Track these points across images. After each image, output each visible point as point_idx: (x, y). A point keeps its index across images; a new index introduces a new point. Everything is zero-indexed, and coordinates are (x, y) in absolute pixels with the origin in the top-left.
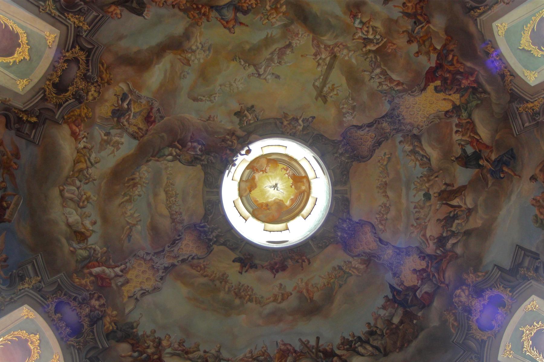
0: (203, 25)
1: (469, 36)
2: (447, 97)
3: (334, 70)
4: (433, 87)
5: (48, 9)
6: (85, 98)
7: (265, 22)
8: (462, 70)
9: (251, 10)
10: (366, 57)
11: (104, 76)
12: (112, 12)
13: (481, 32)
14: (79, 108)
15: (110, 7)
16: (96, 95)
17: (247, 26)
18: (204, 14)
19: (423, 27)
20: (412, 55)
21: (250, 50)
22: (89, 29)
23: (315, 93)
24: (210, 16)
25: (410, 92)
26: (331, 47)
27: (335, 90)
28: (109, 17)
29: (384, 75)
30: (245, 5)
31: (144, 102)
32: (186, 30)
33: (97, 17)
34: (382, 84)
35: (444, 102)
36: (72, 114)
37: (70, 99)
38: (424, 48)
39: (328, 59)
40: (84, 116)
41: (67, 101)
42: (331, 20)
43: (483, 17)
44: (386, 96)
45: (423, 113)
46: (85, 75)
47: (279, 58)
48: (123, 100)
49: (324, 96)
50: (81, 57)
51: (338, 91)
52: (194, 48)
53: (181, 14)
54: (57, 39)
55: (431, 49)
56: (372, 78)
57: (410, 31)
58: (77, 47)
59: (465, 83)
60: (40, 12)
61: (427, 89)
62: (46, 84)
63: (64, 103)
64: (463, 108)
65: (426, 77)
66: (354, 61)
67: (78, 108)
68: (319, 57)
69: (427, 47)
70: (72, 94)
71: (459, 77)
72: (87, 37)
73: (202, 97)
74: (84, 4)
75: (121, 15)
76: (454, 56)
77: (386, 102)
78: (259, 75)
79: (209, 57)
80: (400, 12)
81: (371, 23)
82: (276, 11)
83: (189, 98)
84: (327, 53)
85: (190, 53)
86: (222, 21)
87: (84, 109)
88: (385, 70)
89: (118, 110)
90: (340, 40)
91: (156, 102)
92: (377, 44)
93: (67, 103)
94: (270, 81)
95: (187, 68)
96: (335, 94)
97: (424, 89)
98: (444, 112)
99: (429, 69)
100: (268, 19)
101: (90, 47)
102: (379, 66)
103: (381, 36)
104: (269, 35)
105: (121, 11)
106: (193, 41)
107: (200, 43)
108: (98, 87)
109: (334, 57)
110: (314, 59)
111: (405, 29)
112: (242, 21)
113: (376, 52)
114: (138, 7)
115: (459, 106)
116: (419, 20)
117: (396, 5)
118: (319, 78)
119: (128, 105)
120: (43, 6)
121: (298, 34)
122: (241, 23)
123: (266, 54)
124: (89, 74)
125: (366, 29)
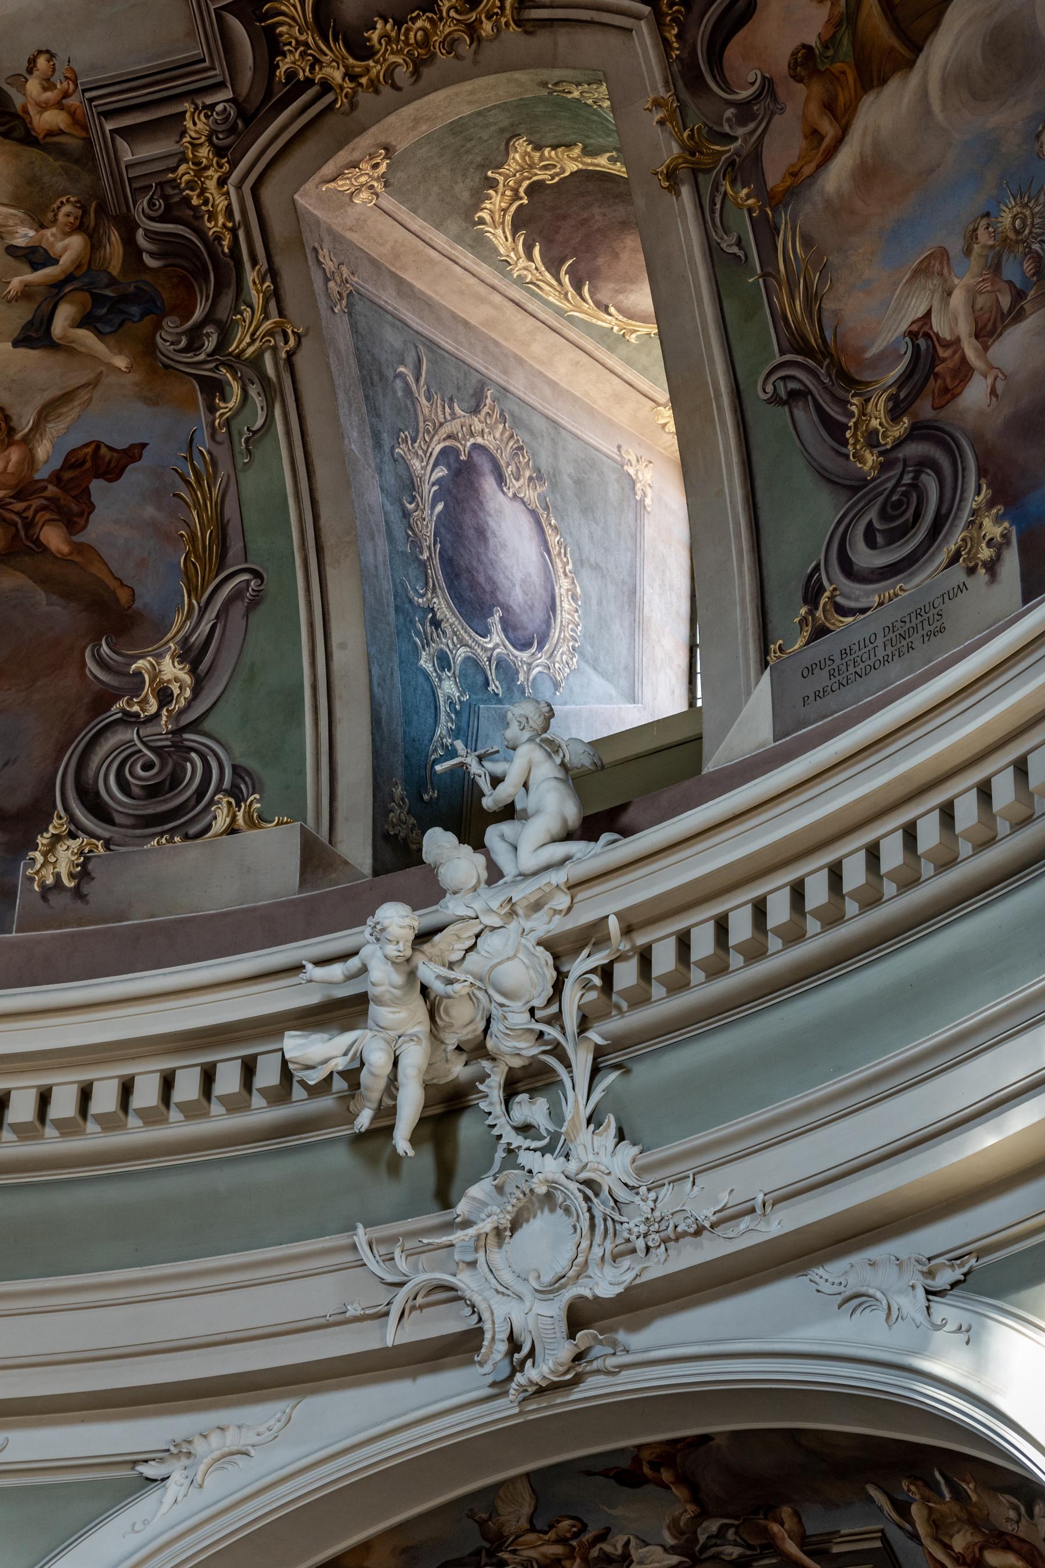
5: (267, 325)
12: (59, 105)
15: (50, 133)
22: (187, 106)
28: (84, 91)
50: (298, 15)
54: (328, 169)
58: (280, 73)
60: (299, 337)
62: (497, 26)
72: (220, 79)
74: (139, 226)
75: (32, 62)
101: (235, 24)
105: (19, 80)
120: (275, 349)
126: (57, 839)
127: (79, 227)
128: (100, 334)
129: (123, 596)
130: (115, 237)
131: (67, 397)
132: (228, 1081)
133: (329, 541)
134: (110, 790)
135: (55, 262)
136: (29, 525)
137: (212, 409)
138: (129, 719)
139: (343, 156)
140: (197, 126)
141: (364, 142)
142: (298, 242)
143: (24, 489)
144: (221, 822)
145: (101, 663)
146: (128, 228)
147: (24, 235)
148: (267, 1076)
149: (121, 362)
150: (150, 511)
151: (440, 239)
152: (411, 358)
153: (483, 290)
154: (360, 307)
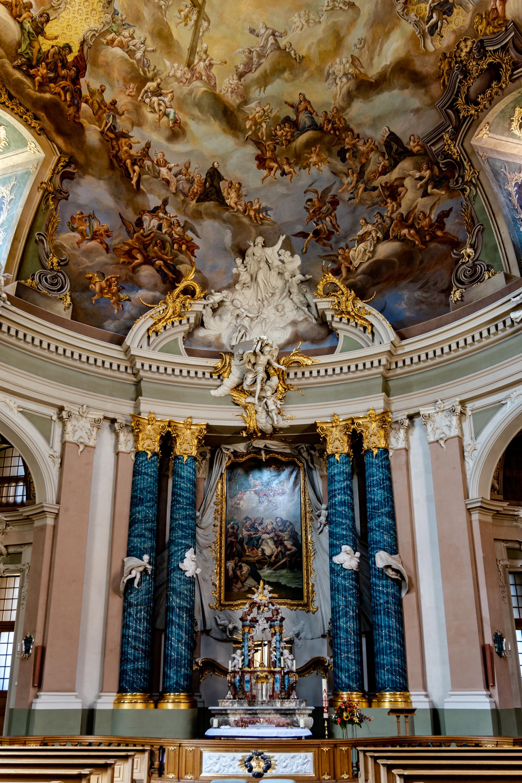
0: (332, 107)
1: (60, 132)
2: (54, 43)
3: (188, 47)
4: (74, 50)
6: (475, 46)
7: (267, 107)
8: (52, 85)
9: (282, 122)
10: (155, 71)
11: (447, 68)
12: (418, 145)
13: (51, 141)
14: (485, 34)
15: (417, 152)
16: (462, 45)
17: (286, 103)
18: (329, 121)
19: (106, 126)
20: (107, 87)
21: (283, 70)
22: (443, 133)
23: (207, 9)
24: (323, 118)
25: (97, 35)
26: (194, 78)
27: (183, 17)
29: (131, 50)
30: (287, 129)
31: (412, 15)
32: (349, 105)
33: (432, 145)
34: (130, 37)
35: (56, 34)
36: (495, 31)
37: (490, 51)
38: (98, 100)
39: (196, 61)
40: (484, 20)
41: (495, 51)
42: (199, 114)
43: (55, 159)
44: (122, 21)
45: (74, 9)
46: (465, 78)
47: (251, 59)
48: (435, 26)
49: (195, 6)
50: (462, 103)
51: (179, 16)
52: (344, 80)
53: (352, 126)
55: (91, 100)
56: (143, 43)
57: (117, 116)
58: (461, 117)
59: (42, 70)
60: (478, 172)
61: (79, 45)
62: (506, 84)
63: (498, 49)
64: (33, 34)
65: (85, 61)
66: (168, 63)
67: (487, 35)
68: (207, 62)
69: (95, 102)
70: (486, 57)
71: (52, 75)
73: (344, 7)
75: (410, 138)
76: (66, 100)
77: (120, 12)
78: (273, 34)
79: (329, 64)
80: (132, 137)
81: (158, 116)
82: (256, 121)
83: (359, 10)
84: (198, 70)
85: (349, 73)
86: (312, 111)
87: (481, 31)
88: (131, 58)
89: (444, 13)
90: (186, 89)
91: (399, 11)
92: (146, 92)
93: (496, 48)
94: (261, 25)
95: (356, 53)
96: (182, 11)
97: (82, 44)
98: (51, 18)
99: (85, 73)
100: (264, 111)
101: (450, 111)
102: (138, 61)
103: (144, 102)
104: (262, 89)
105: (408, 143)
106: (344, 90)
107: (337, 84)
108: (457, 55)
109: (190, 65)
110: (212, 59)
111: (123, 117)
112: (291, 109)
113: (145, 80)
114: (392, 143)
115: (38, 34)
116: (112, 132)
117: (138, 145)
118: (204, 32)
119: (432, 17)
121: (232, 92)
122: (292, 106)
123: (266, 64)
124: (460, 77)
125: (162, 108)
126: (455, 291)
127: (428, 168)
128: (438, 189)
129: (456, 239)
130: (436, 167)
131: (434, 204)
132: (501, 326)
133: (495, 212)
134: (463, 278)
135: (424, 178)
136: (434, 232)
137: (464, 194)
138: (463, 263)
139: (479, 129)
140: (446, 137)
141: (482, 124)
142: (473, 152)
143: (431, 225)
144: (487, 277)
145: (455, 254)
146: (437, 164)
147: (418, 175)
148: (509, 323)
149: (443, 193)
150: (457, 220)
151: (504, 138)
152: (503, 167)
153: (516, 145)
154: (490, 160)
